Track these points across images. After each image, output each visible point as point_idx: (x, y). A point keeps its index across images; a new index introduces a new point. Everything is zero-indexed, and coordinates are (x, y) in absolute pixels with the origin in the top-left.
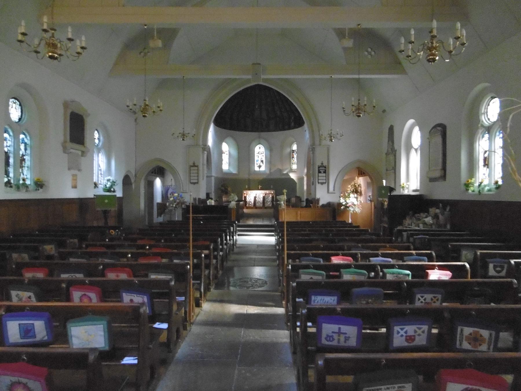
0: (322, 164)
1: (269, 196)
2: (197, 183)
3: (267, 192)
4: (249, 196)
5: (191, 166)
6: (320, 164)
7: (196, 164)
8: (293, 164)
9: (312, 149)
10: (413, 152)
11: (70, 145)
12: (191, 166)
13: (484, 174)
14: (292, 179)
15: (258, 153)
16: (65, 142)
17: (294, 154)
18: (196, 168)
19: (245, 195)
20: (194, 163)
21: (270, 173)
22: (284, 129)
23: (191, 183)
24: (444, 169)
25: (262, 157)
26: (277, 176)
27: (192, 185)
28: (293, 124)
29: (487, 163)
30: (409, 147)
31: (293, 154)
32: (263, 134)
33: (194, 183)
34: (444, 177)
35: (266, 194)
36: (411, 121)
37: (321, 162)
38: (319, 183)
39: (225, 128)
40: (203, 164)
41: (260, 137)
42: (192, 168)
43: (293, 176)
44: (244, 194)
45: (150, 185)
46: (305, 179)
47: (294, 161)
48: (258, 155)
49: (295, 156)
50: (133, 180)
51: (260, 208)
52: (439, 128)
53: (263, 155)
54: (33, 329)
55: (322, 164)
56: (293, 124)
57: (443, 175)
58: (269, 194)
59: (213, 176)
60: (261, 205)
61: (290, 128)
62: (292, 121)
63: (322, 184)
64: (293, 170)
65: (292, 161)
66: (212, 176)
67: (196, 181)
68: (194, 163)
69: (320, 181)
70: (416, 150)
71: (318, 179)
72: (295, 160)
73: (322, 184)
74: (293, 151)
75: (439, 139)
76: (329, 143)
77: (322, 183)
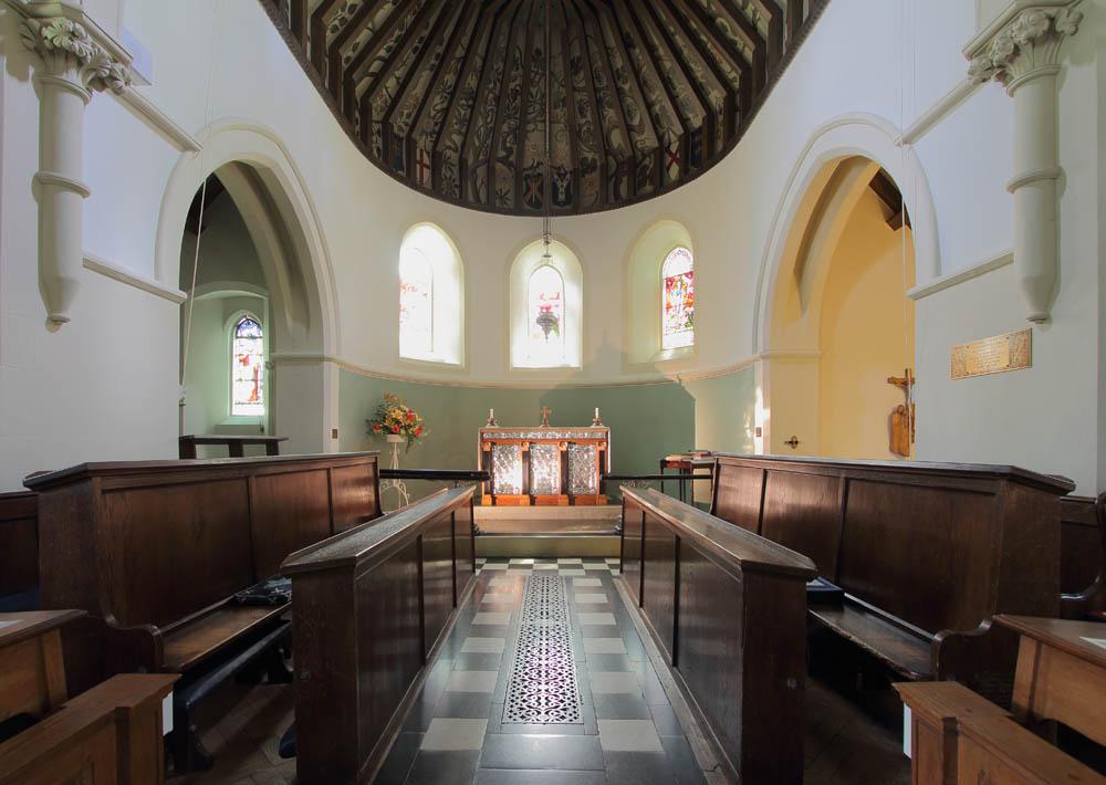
19: (487, 448)
22: (635, 197)
26: (612, 375)
28: (674, 172)
32: (558, 222)
39: (410, 181)
51: (551, 501)
53: (556, 302)
56: (674, 172)
59: (330, 360)
60: (555, 482)
61: (662, 187)
66: (321, 359)
74: (670, 282)
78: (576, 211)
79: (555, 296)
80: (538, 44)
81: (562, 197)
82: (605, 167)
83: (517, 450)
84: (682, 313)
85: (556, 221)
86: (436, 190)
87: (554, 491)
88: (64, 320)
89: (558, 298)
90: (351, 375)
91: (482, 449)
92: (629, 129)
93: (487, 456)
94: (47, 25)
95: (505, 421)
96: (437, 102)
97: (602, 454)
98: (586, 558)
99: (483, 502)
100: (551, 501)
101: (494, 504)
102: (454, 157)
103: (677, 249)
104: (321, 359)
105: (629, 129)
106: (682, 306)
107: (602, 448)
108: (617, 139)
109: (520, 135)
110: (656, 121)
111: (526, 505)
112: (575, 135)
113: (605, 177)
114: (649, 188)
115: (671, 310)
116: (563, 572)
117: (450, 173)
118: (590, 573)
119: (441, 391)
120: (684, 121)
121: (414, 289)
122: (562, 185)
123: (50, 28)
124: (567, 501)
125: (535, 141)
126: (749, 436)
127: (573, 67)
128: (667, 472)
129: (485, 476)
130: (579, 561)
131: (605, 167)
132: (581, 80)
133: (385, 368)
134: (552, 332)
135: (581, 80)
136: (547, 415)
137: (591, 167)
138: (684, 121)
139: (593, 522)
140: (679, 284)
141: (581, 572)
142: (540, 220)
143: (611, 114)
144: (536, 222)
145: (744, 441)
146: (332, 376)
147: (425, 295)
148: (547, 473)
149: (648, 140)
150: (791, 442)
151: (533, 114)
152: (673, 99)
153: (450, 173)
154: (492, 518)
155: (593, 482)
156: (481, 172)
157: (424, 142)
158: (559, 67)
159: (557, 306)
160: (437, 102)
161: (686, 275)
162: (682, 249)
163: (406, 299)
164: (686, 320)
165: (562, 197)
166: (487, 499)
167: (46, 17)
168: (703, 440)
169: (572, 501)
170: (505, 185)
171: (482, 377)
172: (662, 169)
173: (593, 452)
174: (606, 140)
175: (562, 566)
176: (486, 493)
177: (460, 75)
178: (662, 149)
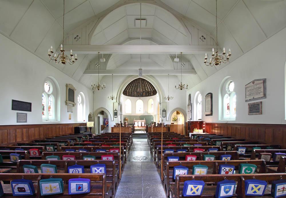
3: (142, 120)
6: (163, 110)
10: (198, 104)
11: (68, 102)
13: (228, 113)
16: (67, 100)
24: (212, 111)
26: (146, 114)
27: (115, 118)
29: (228, 108)
30: (197, 102)
34: (211, 114)
36: (198, 92)
39: (127, 95)
40: (119, 110)
41: (140, 99)
45: (99, 118)
50: (92, 116)
51: (140, 127)
52: (210, 95)
54: (82, 188)
57: (211, 113)
60: (141, 126)
61: (151, 95)
70: (200, 103)
75: (210, 99)
76: (167, 101)
77: (164, 117)
78: (143, 97)
80: (139, 81)
82: (146, 92)
83: (137, 122)
85: (141, 98)
86: (129, 96)
90: (124, 115)
92: (148, 89)
93: (134, 123)
95: (136, 120)
96: (129, 87)
100: (140, 127)
102: (130, 91)
105: (148, 89)
108: (147, 90)
109: (137, 89)
110: (150, 89)
112: (143, 89)
113: (146, 93)
114: (150, 95)
117: (130, 93)
119: (130, 117)
120: (153, 90)
122: (141, 94)
125: (138, 90)
127: (142, 83)
131: (146, 92)
132: (143, 84)
135: (143, 84)
137: (144, 92)
138: (153, 90)
143: (146, 87)
148: (140, 125)
149: (149, 90)
151: (138, 87)
152: (151, 87)
153: (130, 93)
156: (133, 92)
157: (128, 91)
158: (141, 83)
160: (129, 87)
169: (142, 127)
170: (135, 94)
171: (133, 115)
172: (151, 93)
173: (144, 122)
174: (146, 89)
177: (132, 85)
178: (151, 91)
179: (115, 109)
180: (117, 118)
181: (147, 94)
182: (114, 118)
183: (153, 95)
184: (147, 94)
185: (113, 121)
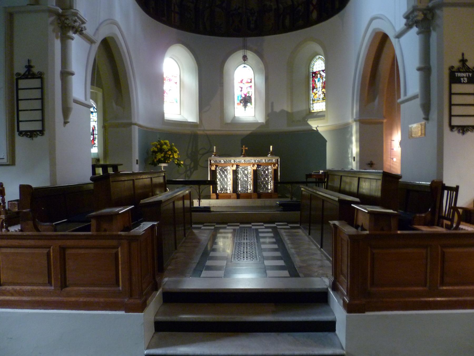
0: (463, 61)
1: (268, 169)
2: (42, 132)
3: (263, 160)
4: (221, 170)
5: (21, 77)
6: (457, 64)
7: (35, 70)
8: (313, 100)
9: (425, 15)
12: (21, 77)
14: (317, 132)
15: (242, 82)
17: (317, 80)
18: (36, 83)
19: (213, 168)
20: (29, 67)
21: (267, 122)
22: (294, 27)
23: (21, 133)
25: (249, 89)
28: (315, 15)
31: (314, 81)
32: (251, 40)
33: (31, 134)
35: (259, 166)
37: (460, 58)
38: (452, 127)
39: (169, 22)
41: (245, 47)
42: (23, 83)
43: (314, 124)
44: (211, 165)
46: (355, 128)
47: (317, 95)
48: (241, 85)
49: (319, 84)
51: (248, 196)
53: (250, 84)
55: (463, 61)
56: (315, 15)
58: (267, 164)
59: (135, 124)
60: (250, 188)
61: (308, 23)
62: (312, 8)
63: (463, 133)
64: (315, 114)
65: (312, 95)
67: (37, 126)
68: (29, 67)
69: (456, 121)
71: (451, 116)
72: (319, 92)
73: (463, 133)
79: (249, 81)
81: (252, 26)
84: (321, 93)
85: (249, 39)
87: (249, 191)
88: (68, 122)
89: (251, 82)
91: (210, 169)
93: (214, 173)
94: (67, 19)
97: (275, 171)
98: (265, 223)
99: (211, 197)
101: (217, 198)
103: (318, 57)
104: (131, 124)
106: (321, 89)
107: (275, 168)
111: (234, 198)
115: (315, 90)
116: (253, 227)
118: (266, 228)
121: (170, 80)
123: (68, 20)
124: (257, 196)
126: (350, 161)
128: (310, 180)
129: (213, 182)
130: (262, 224)
133: (157, 126)
134: (249, 104)
136: (245, 150)
139: (270, 207)
140: (319, 76)
141: (263, 227)
142: (241, 39)
144: (239, 40)
145: (348, 163)
146: (136, 133)
147: (176, 83)
150: (369, 164)
154: (216, 206)
155: (270, 186)
159: (251, 87)
161: (323, 71)
162: (320, 56)
163: (167, 86)
164: (322, 96)
165: (252, 26)
166: (214, 195)
167: (67, 15)
168: (330, 165)
173: (271, 169)
175: (253, 225)
176: (213, 192)
179: (20, 68)
180: (39, 139)
181: (287, 22)
182: (20, 141)
183: (321, 19)
184: (287, 22)
185: (12, 162)
